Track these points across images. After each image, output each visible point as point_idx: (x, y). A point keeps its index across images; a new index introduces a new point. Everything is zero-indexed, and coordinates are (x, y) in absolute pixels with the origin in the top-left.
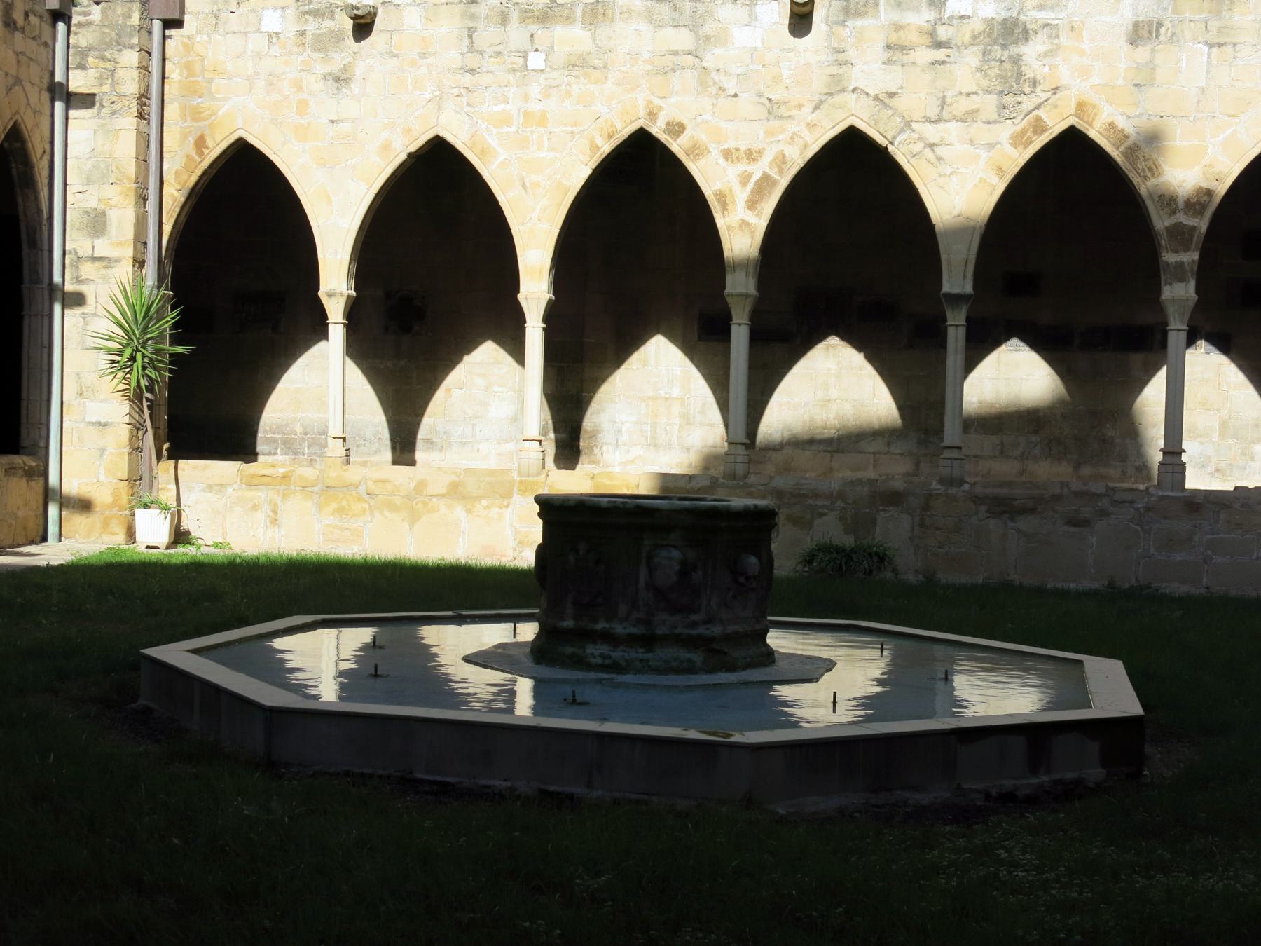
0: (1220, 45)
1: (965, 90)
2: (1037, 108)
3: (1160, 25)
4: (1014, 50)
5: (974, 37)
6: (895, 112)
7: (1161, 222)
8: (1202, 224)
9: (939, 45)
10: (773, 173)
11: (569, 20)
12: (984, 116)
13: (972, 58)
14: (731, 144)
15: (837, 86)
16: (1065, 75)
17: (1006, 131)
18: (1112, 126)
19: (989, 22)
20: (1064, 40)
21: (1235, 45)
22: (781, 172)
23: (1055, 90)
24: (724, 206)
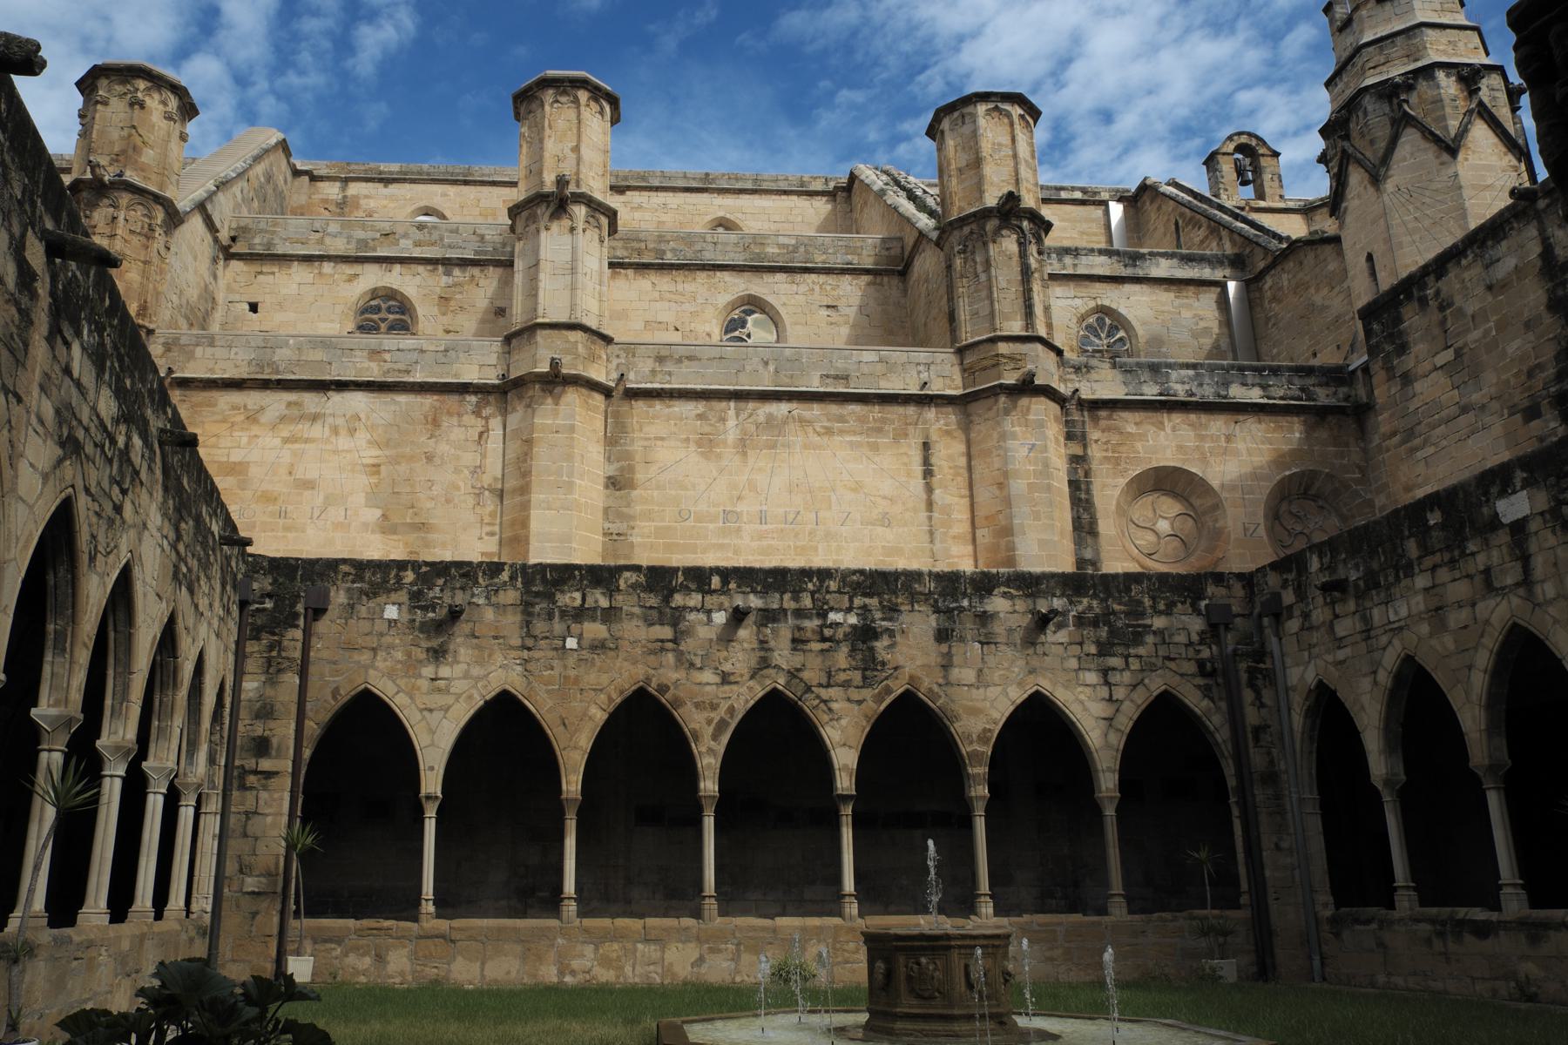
0: (988, 643)
1: (843, 667)
2: (886, 678)
3: (953, 630)
4: (869, 644)
5: (845, 635)
6: (801, 680)
7: (965, 749)
8: (988, 750)
9: (824, 639)
10: (727, 718)
11: (594, 619)
12: (855, 683)
13: (844, 649)
14: (699, 699)
15: (764, 663)
16: (901, 660)
17: (867, 693)
18: (930, 690)
19: (853, 627)
20: (898, 638)
21: (996, 644)
22: (732, 717)
23: (896, 668)
24: (696, 739)
